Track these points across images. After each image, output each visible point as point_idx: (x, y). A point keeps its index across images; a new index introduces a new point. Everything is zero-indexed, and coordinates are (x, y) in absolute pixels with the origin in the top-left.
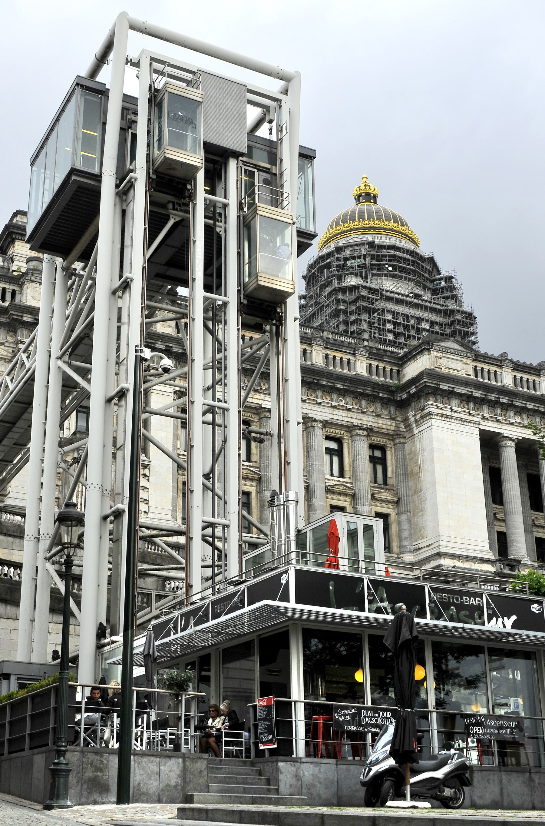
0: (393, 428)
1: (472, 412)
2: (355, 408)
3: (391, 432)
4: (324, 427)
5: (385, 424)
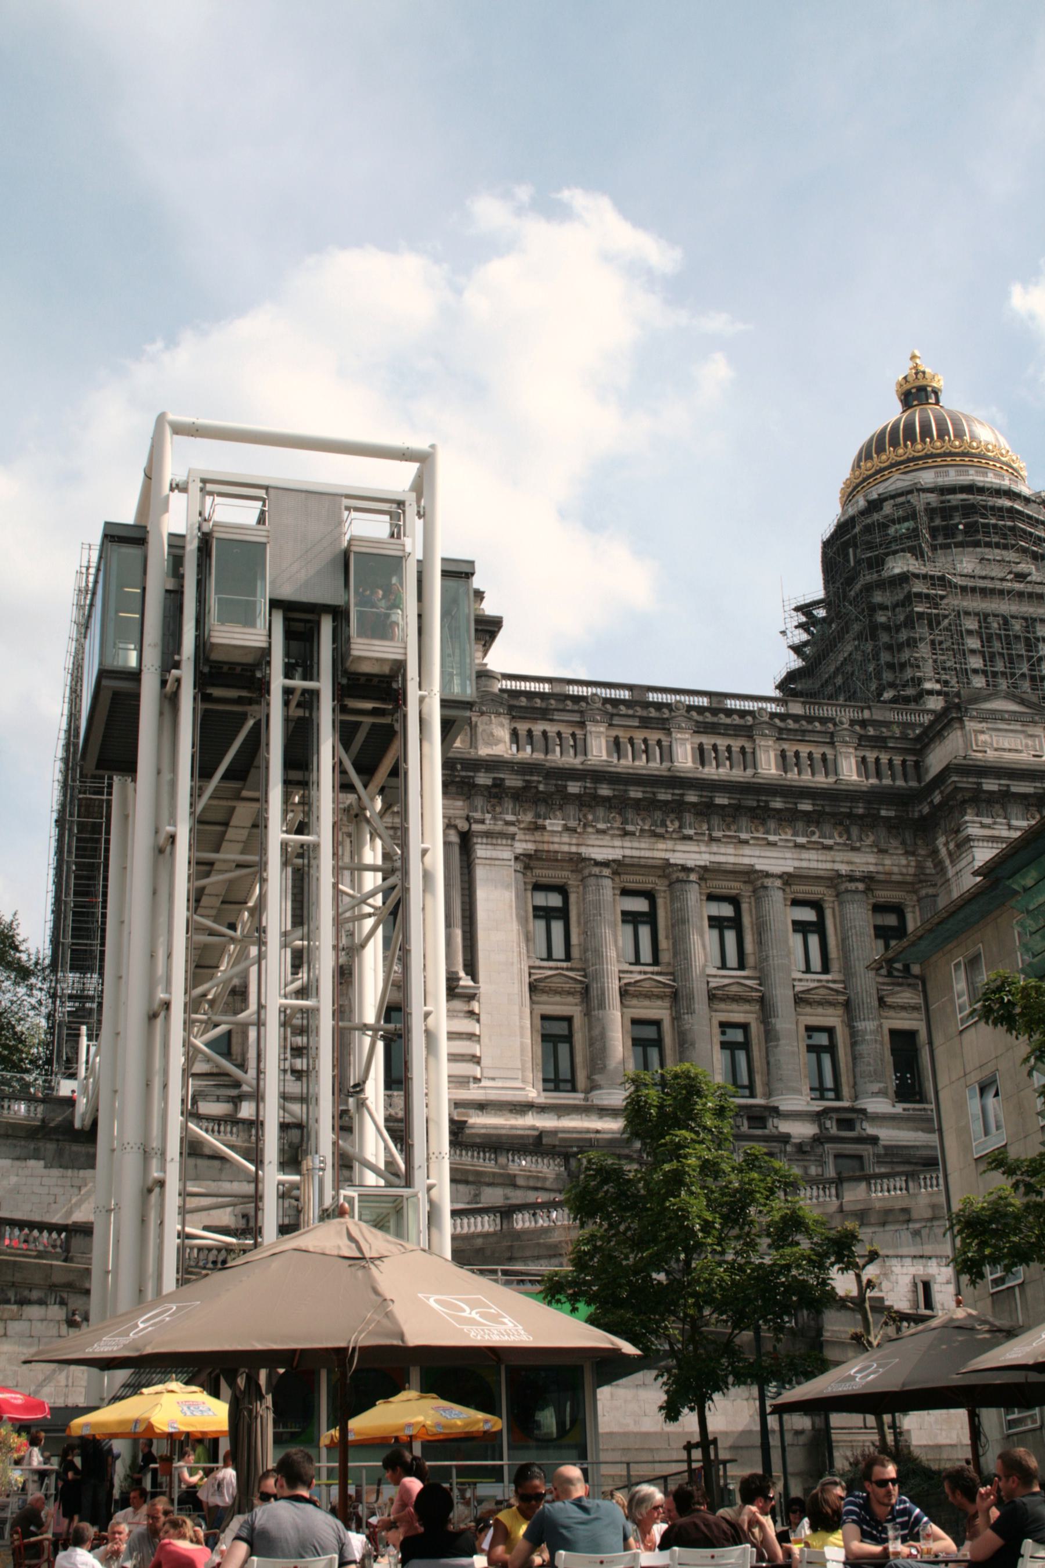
2: (838, 844)
3: (909, 879)
4: (786, 883)
5: (896, 863)
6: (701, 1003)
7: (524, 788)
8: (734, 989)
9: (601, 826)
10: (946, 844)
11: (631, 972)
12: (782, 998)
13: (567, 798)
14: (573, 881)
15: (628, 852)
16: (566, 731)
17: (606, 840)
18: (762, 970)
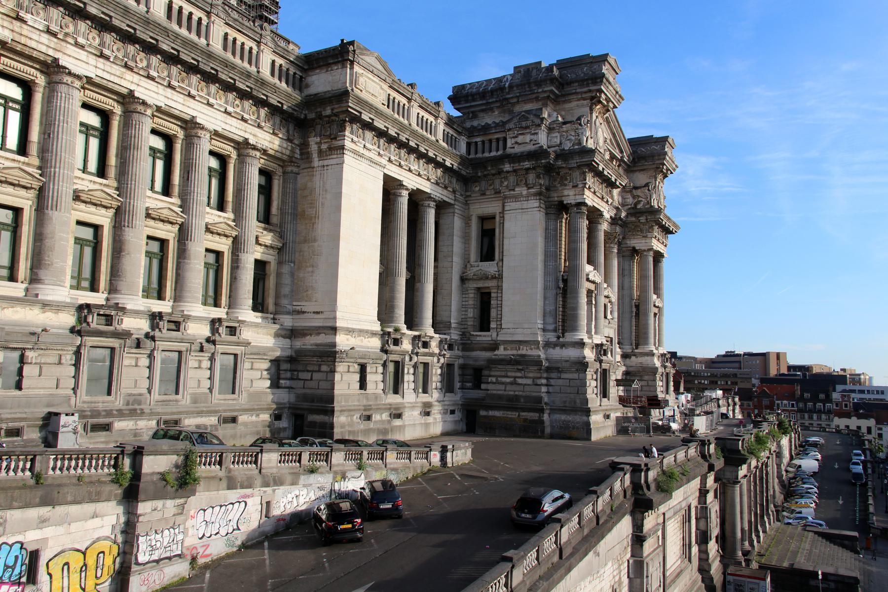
0: (288, 153)
1: (382, 152)
3: (285, 157)
9: (81, 40)
10: (320, 143)
11: (83, 179)
17: (83, 55)
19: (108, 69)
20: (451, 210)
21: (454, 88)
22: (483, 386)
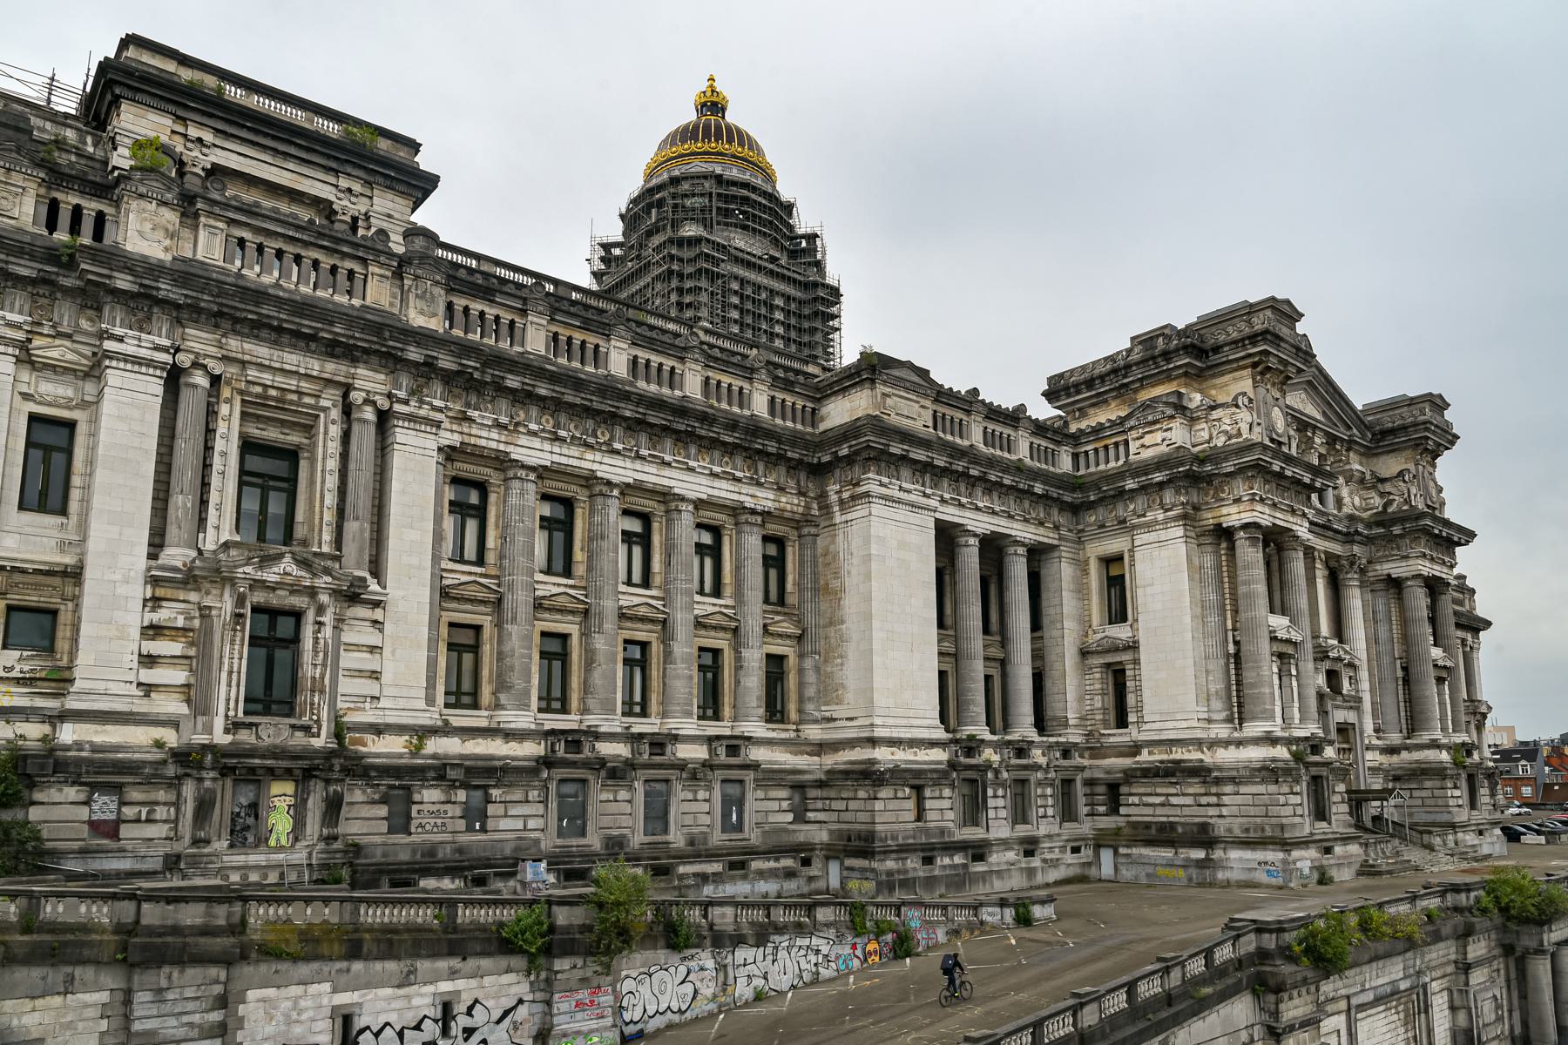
0: (801, 510)
1: (929, 491)
3: (797, 517)
4: (696, 508)
5: (791, 503)
6: (609, 626)
7: (458, 373)
8: (643, 611)
9: (533, 427)
10: (840, 492)
12: (682, 623)
13: (501, 389)
14: (494, 478)
15: (556, 458)
16: (507, 317)
17: (536, 443)
18: (667, 591)
19: (565, 451)
20: (1056, 554)
21: (1050, 379)
22: (1123, 810)
